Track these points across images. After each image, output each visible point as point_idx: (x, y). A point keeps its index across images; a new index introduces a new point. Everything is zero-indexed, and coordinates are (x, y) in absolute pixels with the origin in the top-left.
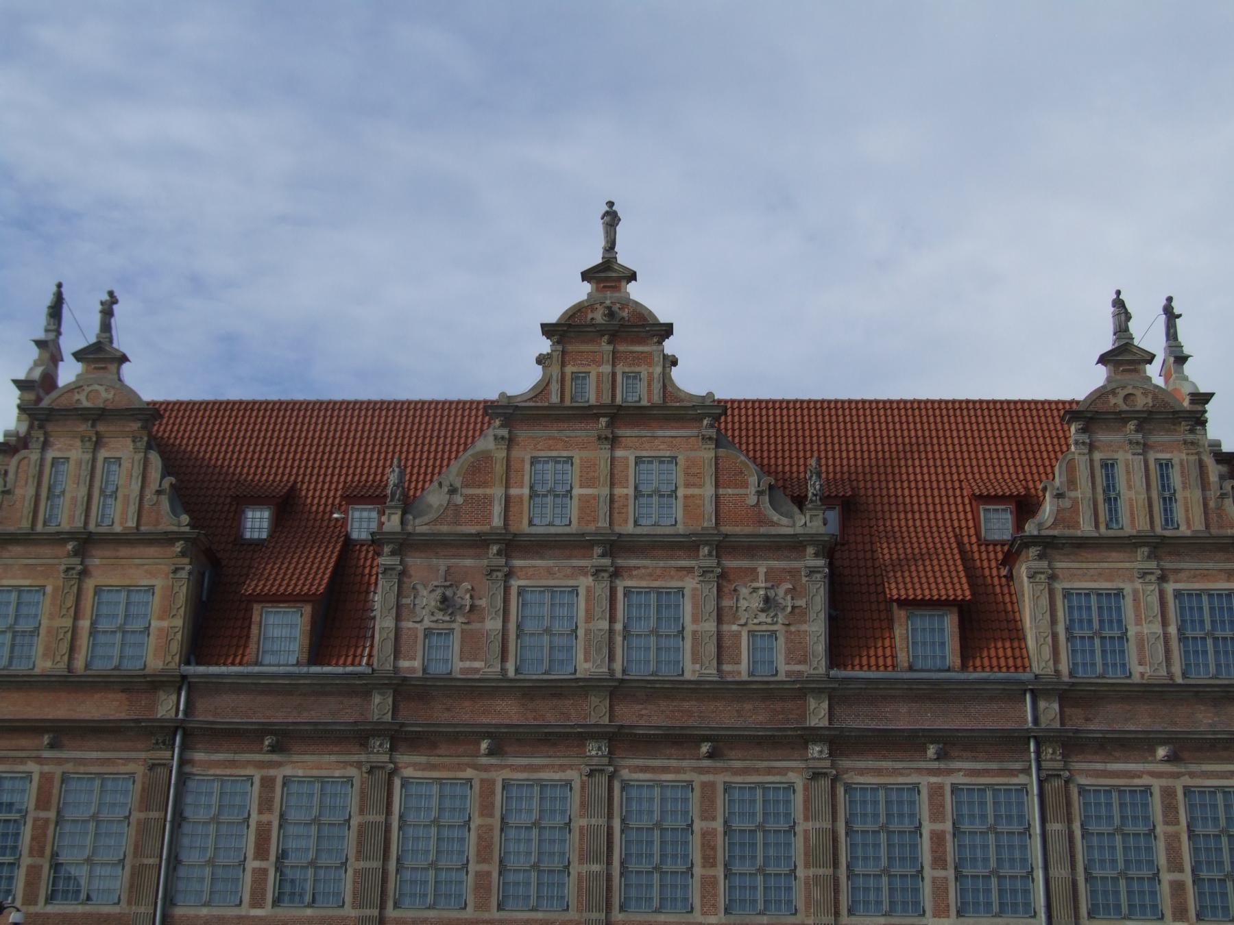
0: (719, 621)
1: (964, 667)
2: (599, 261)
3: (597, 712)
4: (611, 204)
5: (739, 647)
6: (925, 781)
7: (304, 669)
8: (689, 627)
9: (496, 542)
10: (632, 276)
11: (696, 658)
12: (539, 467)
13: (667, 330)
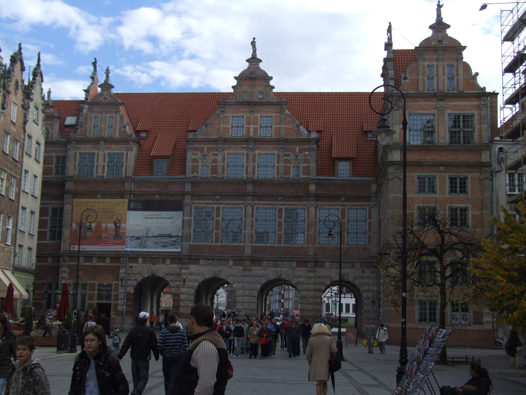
0: (285, 163)
1: (354, 177)
2: (251, 56)
3: (250, 188)
4: (254, 39)
5: (290, 171)
6: (340, 208)
7: (166, 177)
8: (276, 165)
9: (220, 141)
10: (261, 61)
11: (278, 174)
12: (234, 119)
13: (271, 78)
